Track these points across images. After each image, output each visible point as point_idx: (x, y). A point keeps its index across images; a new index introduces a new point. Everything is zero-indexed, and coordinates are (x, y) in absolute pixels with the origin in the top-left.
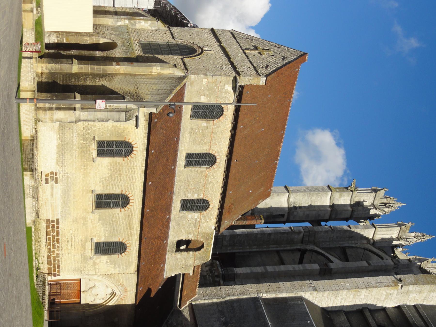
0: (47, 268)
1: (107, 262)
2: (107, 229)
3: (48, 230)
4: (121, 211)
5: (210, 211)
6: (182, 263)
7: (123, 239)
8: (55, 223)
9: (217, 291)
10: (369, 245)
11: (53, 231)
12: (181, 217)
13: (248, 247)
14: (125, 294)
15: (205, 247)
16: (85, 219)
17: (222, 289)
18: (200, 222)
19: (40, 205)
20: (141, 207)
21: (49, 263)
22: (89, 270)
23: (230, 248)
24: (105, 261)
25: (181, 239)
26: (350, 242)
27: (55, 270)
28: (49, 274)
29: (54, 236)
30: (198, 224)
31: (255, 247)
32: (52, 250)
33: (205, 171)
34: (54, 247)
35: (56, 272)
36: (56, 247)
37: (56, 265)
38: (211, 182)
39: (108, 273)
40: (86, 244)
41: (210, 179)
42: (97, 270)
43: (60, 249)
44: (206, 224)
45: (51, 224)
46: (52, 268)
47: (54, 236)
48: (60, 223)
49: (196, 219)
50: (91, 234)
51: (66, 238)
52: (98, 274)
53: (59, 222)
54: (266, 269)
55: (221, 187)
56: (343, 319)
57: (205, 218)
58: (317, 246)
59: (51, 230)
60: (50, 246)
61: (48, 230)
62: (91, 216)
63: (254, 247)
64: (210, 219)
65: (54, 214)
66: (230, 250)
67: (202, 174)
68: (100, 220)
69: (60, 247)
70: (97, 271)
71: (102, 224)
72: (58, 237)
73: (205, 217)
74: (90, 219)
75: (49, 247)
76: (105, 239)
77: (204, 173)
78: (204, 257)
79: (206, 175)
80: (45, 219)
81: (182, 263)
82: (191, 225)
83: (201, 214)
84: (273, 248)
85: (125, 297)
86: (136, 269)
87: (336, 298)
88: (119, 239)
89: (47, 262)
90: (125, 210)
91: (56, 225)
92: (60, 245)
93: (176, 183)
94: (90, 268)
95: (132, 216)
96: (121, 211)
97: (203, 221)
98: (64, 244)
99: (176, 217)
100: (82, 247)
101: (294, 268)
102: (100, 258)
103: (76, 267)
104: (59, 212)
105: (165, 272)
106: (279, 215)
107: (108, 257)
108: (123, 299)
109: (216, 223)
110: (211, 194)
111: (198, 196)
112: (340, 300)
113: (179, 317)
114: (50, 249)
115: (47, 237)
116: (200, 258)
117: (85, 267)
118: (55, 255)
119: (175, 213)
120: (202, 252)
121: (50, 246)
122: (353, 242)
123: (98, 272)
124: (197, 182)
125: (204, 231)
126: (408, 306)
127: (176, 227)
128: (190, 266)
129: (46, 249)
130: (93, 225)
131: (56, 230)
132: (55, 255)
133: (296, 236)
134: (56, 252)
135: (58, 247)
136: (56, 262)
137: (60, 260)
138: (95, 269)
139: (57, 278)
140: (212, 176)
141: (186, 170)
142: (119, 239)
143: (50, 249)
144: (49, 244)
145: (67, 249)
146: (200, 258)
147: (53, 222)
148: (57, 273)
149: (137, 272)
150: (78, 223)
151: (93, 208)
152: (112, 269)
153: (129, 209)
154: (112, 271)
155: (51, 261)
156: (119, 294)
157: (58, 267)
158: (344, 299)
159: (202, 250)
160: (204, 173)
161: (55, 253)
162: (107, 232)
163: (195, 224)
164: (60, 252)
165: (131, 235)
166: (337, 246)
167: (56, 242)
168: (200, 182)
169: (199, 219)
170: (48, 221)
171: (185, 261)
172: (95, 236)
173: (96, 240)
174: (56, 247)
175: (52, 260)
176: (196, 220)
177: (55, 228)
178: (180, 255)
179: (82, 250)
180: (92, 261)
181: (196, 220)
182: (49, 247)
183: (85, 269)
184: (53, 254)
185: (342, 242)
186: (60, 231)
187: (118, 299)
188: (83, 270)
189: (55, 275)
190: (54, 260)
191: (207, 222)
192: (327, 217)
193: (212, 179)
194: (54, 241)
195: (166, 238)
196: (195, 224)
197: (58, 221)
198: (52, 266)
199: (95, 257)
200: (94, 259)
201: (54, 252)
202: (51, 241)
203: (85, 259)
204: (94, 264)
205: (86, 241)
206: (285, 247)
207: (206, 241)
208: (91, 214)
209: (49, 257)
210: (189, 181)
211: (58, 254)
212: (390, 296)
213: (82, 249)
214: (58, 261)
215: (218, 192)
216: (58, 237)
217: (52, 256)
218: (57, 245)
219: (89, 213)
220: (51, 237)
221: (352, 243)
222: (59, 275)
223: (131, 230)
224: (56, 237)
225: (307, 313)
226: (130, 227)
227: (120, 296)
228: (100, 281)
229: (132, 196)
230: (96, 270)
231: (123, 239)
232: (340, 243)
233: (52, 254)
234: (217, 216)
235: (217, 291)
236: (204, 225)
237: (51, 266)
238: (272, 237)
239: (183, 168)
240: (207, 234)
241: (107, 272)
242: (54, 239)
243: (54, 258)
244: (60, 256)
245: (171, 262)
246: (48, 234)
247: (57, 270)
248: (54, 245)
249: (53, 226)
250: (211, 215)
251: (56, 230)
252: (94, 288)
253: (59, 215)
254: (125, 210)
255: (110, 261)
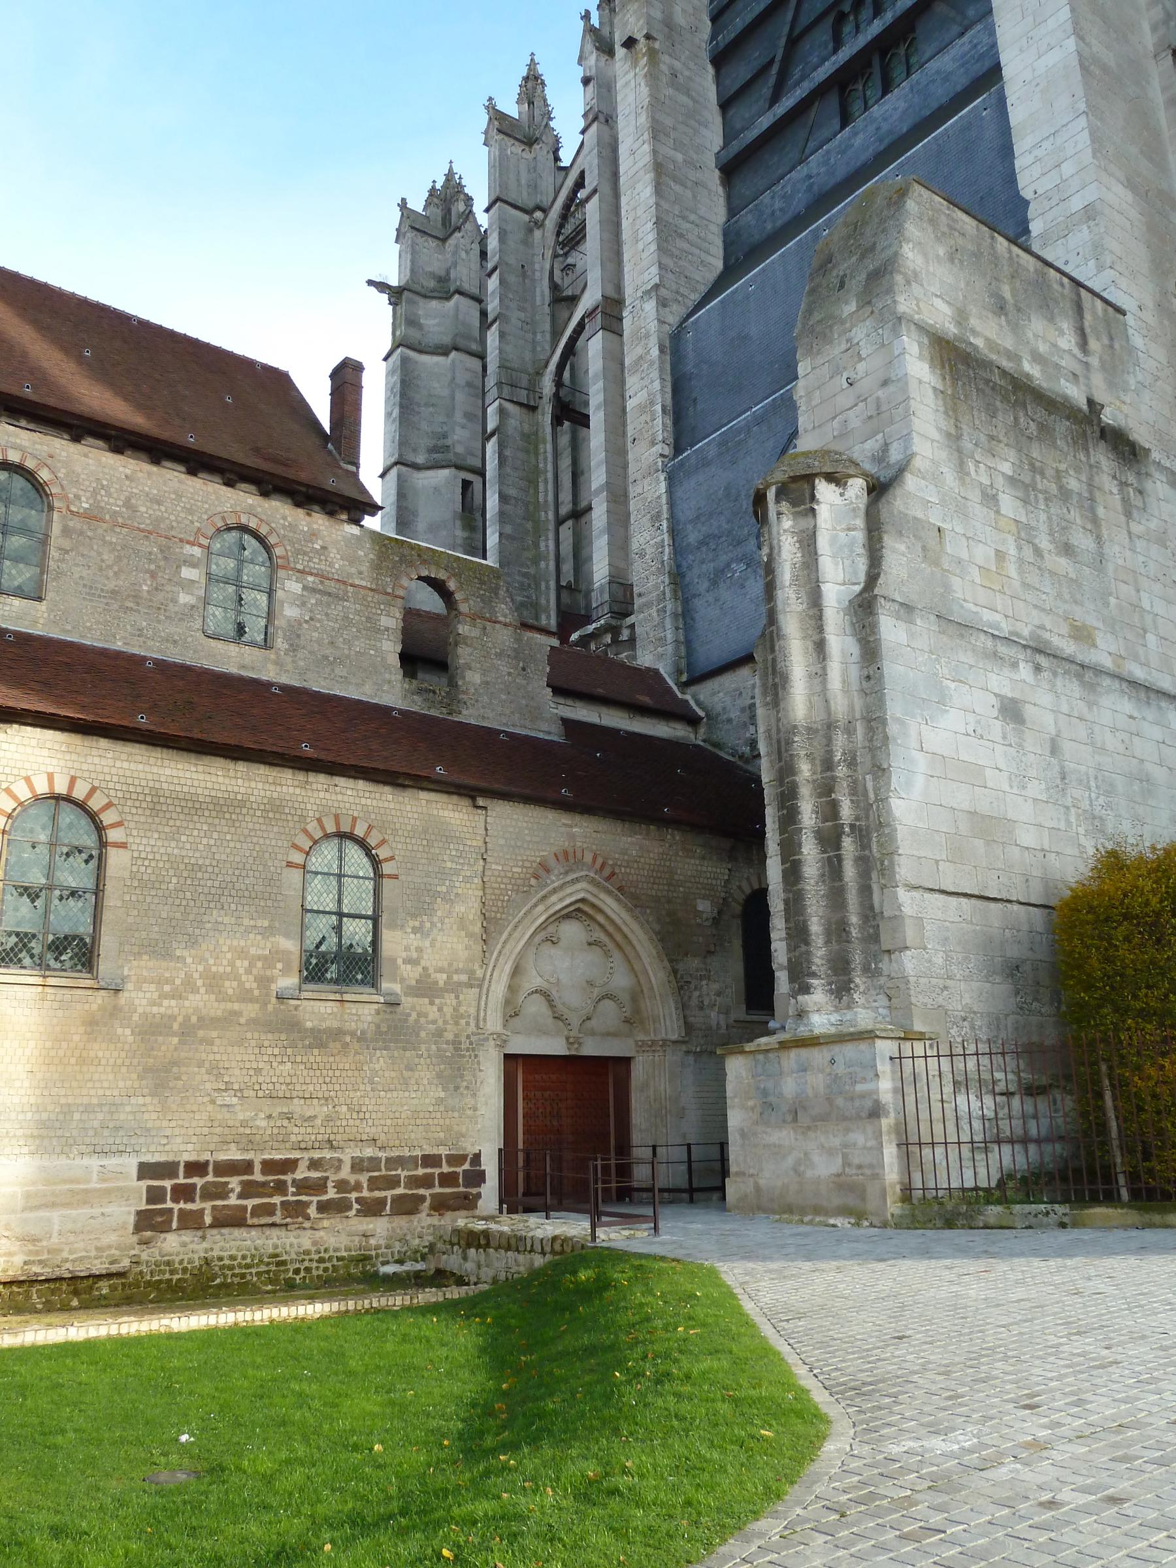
0: (435, 1220)
1: (415, 930)
2: (226, 920)
3: (208, 1220)
4: (123, 846)
5: (272, 530)
6: (505, 670)
7: (295, 846)
8: (168, 1184)
9: (648, 605)
10: (547, 222)
11: (216, 1192)
12: (294, 648)
13: (543, 564)
14: (588, 858)
15: (442, 575)
16: (152, 1029)
17: (642, 590)
18: (322, 576)
19: (36, 1269)
20: (104, 743)
21: (407, 1206)
22: (457, 1016)
23: (543, 617)
24: (414, 940)
25: (394, 660)
26: (537, 274)
27: (448, 1180)
28: (468, 1202)
29: (249, 1190)
30: (333, 584)
31: (542, 545)
32: (331, 1194)
33: (64, 517)
34: (319, 1187)
35: (459, 1170)
36: (315, 1175)
37: (421, 1171)
38: (127, 503)
39: (477, 929)
40: (309, 1025)
41: (114, 503)
42: (455, 978)
43: (328, 1154)
44: (333, 553)
45: (169, 1204)
46: (438, 1190)
47: (249, 1190)
48: (170, 1158)
49: (305, 588)
50: (252, 1000)
51: (263, 1124)
52: (479, 974)
53: (158, 1165)
54: (598, 492)
55: (154, 469)
56: (750, 217)
57: (305, 553)
58: (546, 366)
59: (208, 1205)
60: (307, 1204)
61: (208, 1220)
62: (140, 999)
63: (543, 548)
64: (314, 535)
65: (108, 1192)
66: (548, 617)
67: (81, 533)
68: (160, 950)
69: (317, 1155)
70: (464, 978)
71: (192, 942)
72: (257, 1168)
73: (297, 552)
74: (153, 1003)
75: (312, 1211)
76: (287, 935)
77: (73, 523)
78: (482, 583)
79: (91, 517)
80: (135, 1238)
81: (505, 670)
82: (336, 610)
83: (284, 567)
84: (546, 491)
85: (600, 861)
86: (466, 802)
87: (681, 236)
88: (290, 865)
89: (401, 1222)
90: (119, 824)
91: (181, 1180)
92: (306, 1155)
93: (118, 645)
94: (448, 1010)
95: (156, 793)
96: (123, 846)
97: (316, 564)
98: (297, 1133)
99: (290, 667)
100: (322, 1045)
101: (598, 408)
102: (393, 961)
103: (439, 1076)
104: (95, 1162)
105: (541, 735)
106: (464, 494)
107: (393, 926)
108: (607, 872)
109: (331, 514)
110: (190, 511)
111: (194, 565)
112: (688, 226)
113: (729, 721)
114: (323, 1207)
115: (250, 1222)
116: (487, 602)
117: (439, 1033)
118: (364, 1178)
119: (270, 666)
120: (461, 588)
121: (307, 1204)
122: (537, 266)
123: (472, 973)
124: (119, 559)
125: (365, 567)
126: (713, 37)
127: (340, 671)
128: (518, 640)
129: (326, 1223)
130: (195, 991)
131: (210, 1178)
132: (364, 1178)
133: (513, 423)
134: (345, 1173)
135: (314, 1164)
136: (403, 1174)
137: (395, 1153)
138: (454, 988)
139: (490, 1167)
140: (95, 492)
141: (50, 595)
142: (290, 865)
143: (323, 1207)
144: (296, 1210)
145: (328, 1119)
146: (487, 602)
147: (155, 1195)
148: (466, 1166)
149: (481, 802)
150: (175, 1063)
151: (89, 983)
152: (460, 908)
153: (109, 805)
154: (469, 907)
155: (397, 1200)
156: (583, 885)
157: (430, 1160)
158: (687, 213)
159: (452, 585)
160: (73, 523)
161: (352, 1179)
162: (246, 922)
163: (329, 594)
164: (347, 1156)
165: (274, 808)
166: (547, 310)
167: (288, 1178)
168: (124, 547)
169: (310, 579)
170: (149, 1222)
171: (499, 655)
172: (264, 982)
173: (288, 981)
174: (315, 1175)
175: (389, 1194)
176: (314, 590)
177: (198, 1181)
178: (469, 675)
179: (346, 1046)
180: (407, 1002)
181: (314, 590)
182: (312, 1211)
183: (449, 1036)
184: (358, 1187)
185: (538, 299)
186: (222, 1157)
187: (609, 892)
188: (456, 1043)
189: (477, 1177)
190: (393, 1182)
191: (324, 548)
192: (476, 364)
193: (109, 495)
194: (281, 1188)
195: (383, 711)
196: (329, 594)
197: (146, 1170)
198: (422, 1191)
199: (385, 985)
200: (397, 988)
201: (342, 1186)
202: (277, 1200)
203: (395, 1031)
204: (425, 988)
205: (290, 1027)
206: (546, 459)
207: (411, 564)
208: (123, 998)
209: (372, 1209)
210: (113, 592)
211: (358, 1165)
212: (681, 79)
213: (335, 1046)
214: (393, 1162)
215: (180, 482)
216: (257, 1168)
217: (365, 1193)
218: (301, 1173)
219: (115, 1007)
220: (250, 1203)
221: (542, 269)
222: (477, 1157)
223: (242, 804)
224: (258, 1176)
225: (721, 302)
226: (224, 808)
227: (592, 881)
228: (517, 971)
229: (28, 780)
230: (459, 984)
231: (295, 846)
232: (538, 303)
233: (353, 1196)
234: (298, 505)
235: (648, 605)
236: (337, 564)
237: (422, 1199)
238: (512, 492)
239: (43, 607)
240: (382, 556)
241: (470, 935)
242: (264, 1184)
243: (374, 1184)
244: (369, 1152)
245: (499, 709)
246: (232, 1220)
247: (446, 1169)
248: (304, 1186)
249: (183, 1193)
250: (293, 527)
251: (210, 1178)
252: (554, 994)
253: (112, 1162)
254: (119, 824)
255: (414, 916)
